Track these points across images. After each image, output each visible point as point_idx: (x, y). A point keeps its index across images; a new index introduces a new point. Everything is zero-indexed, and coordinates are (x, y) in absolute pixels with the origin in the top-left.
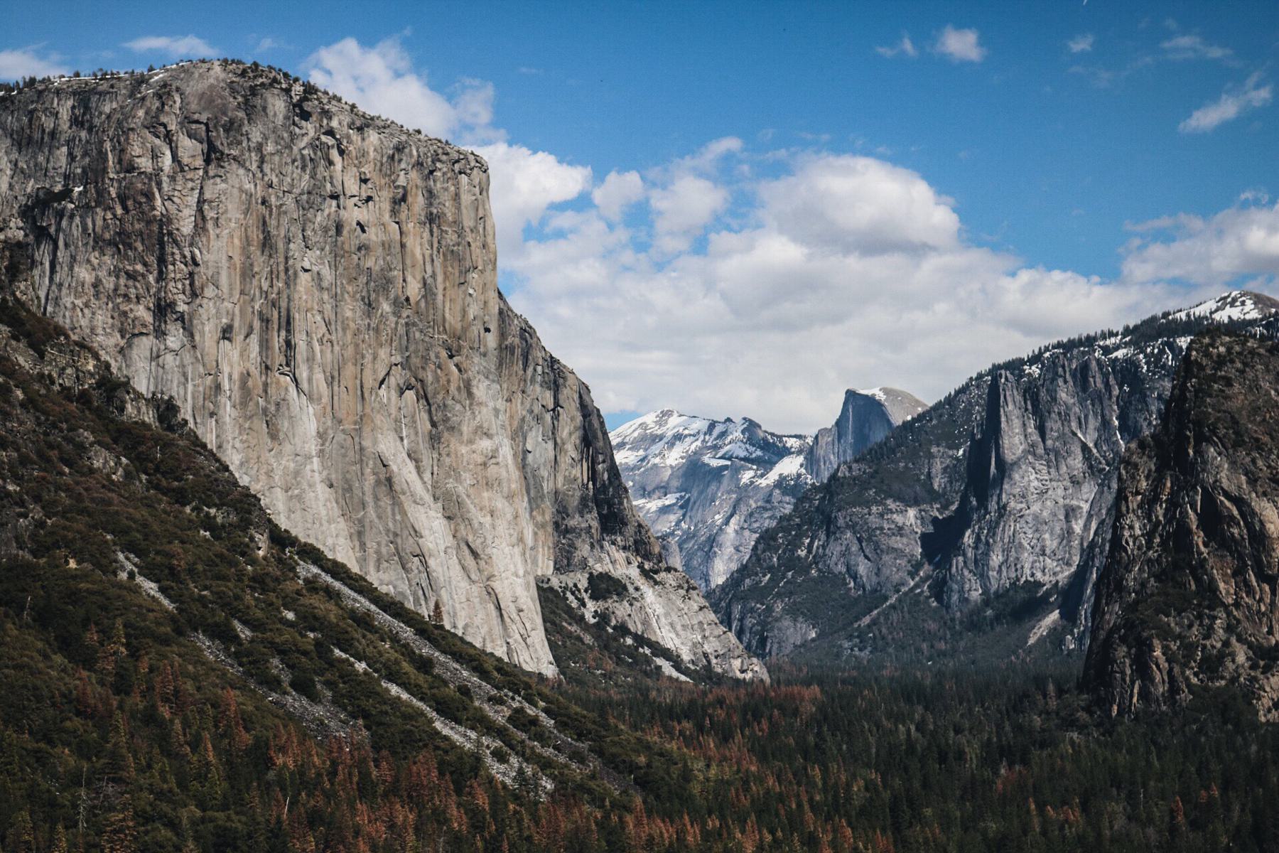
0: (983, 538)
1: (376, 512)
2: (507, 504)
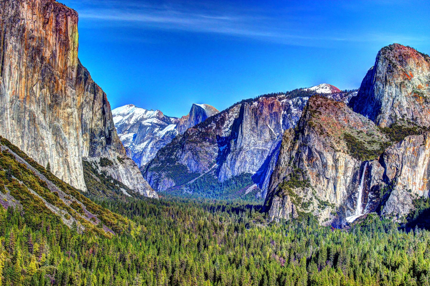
0: (234, 157)
1: (28, 130)
2: (74, 131)
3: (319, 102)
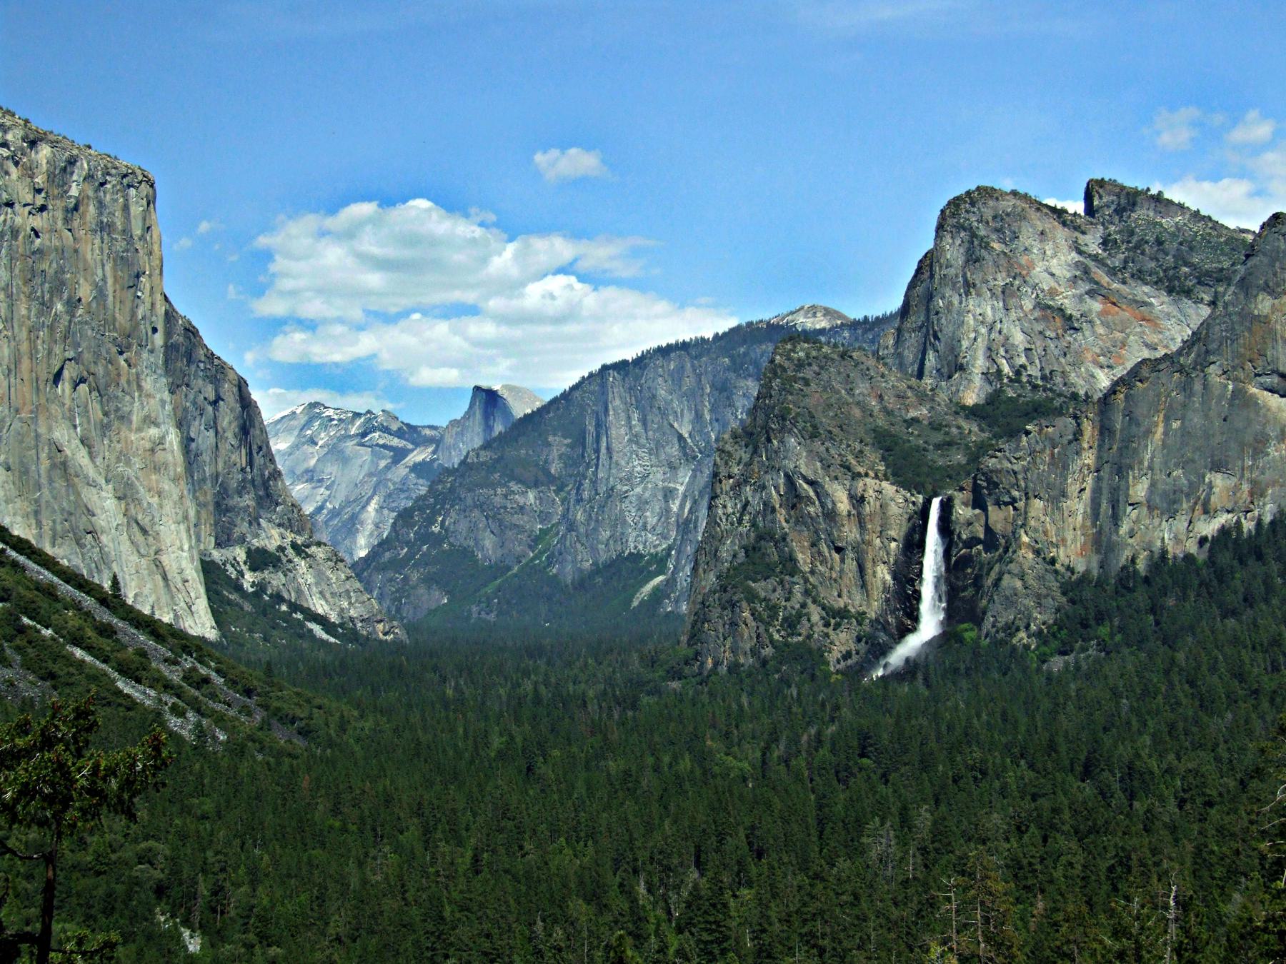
1: (51, 492)
2: (173, 486)
3: (802, 354)
